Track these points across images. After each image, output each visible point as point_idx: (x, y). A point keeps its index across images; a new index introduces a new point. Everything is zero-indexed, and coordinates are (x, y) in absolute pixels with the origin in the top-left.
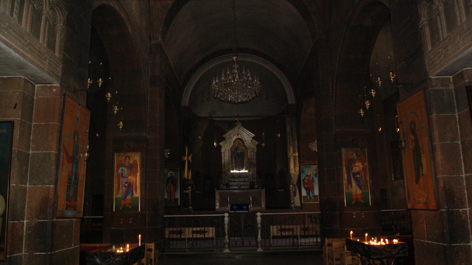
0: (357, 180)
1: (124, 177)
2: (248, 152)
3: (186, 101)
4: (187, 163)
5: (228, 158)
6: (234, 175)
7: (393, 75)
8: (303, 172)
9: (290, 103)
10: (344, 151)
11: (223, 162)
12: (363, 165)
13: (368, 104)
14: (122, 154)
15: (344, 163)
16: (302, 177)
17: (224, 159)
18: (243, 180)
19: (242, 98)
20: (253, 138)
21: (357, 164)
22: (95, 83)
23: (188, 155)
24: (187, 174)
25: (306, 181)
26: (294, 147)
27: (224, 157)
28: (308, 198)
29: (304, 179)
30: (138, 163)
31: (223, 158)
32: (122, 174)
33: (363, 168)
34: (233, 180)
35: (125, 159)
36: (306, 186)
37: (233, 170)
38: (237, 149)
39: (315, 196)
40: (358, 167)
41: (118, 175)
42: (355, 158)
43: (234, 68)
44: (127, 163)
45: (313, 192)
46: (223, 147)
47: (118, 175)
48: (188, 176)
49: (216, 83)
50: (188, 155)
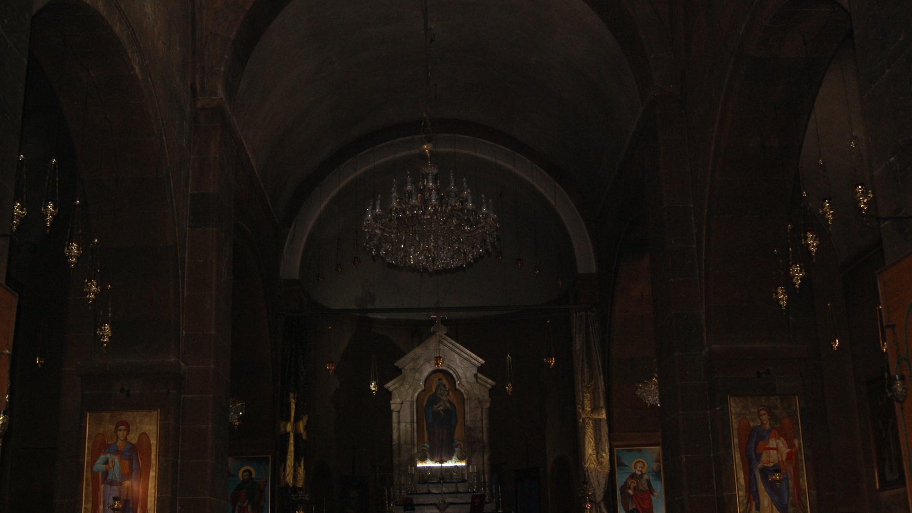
0: (772, 488)
1: (112, 483)
2: (467, 409)
3: (291, 266)
4: (292, 441)
5: (409, 426)
6: (426, 476)
7: (865, 194)
8: (621, 464)
9: (581, 269)
10: (734, 406)
11: (395, 436)
12: (790, 445)
13: (797, 273)
14: (107, 415)
15: (736, 440)
16: (620, 481)
17: (399, 430)
18: (452, 488)
19: (445, 259)
20: (481, 369)
21: (772, 443)
22: (35, 215)
23: (297, 419)
24: (293, 472)
25: (631, 492)
26: (594, 392)
27: (399, 423)
29: (625, 488)
30: (153, 442)
31: (395, 425)
32: (106, 473)
33: (789, 455)
34: (423, 488)
35: (116, 430)
37: (423, 460)
38: (434, 400)
40: (776, 450)
41: (95, 475)
42: (767, 426)
43: (425, 176)
44: (120, 443)
46: (395, 394)
47: (95, 475)
48: (295, 477)
49: (376, 218)
50: (297, 419)
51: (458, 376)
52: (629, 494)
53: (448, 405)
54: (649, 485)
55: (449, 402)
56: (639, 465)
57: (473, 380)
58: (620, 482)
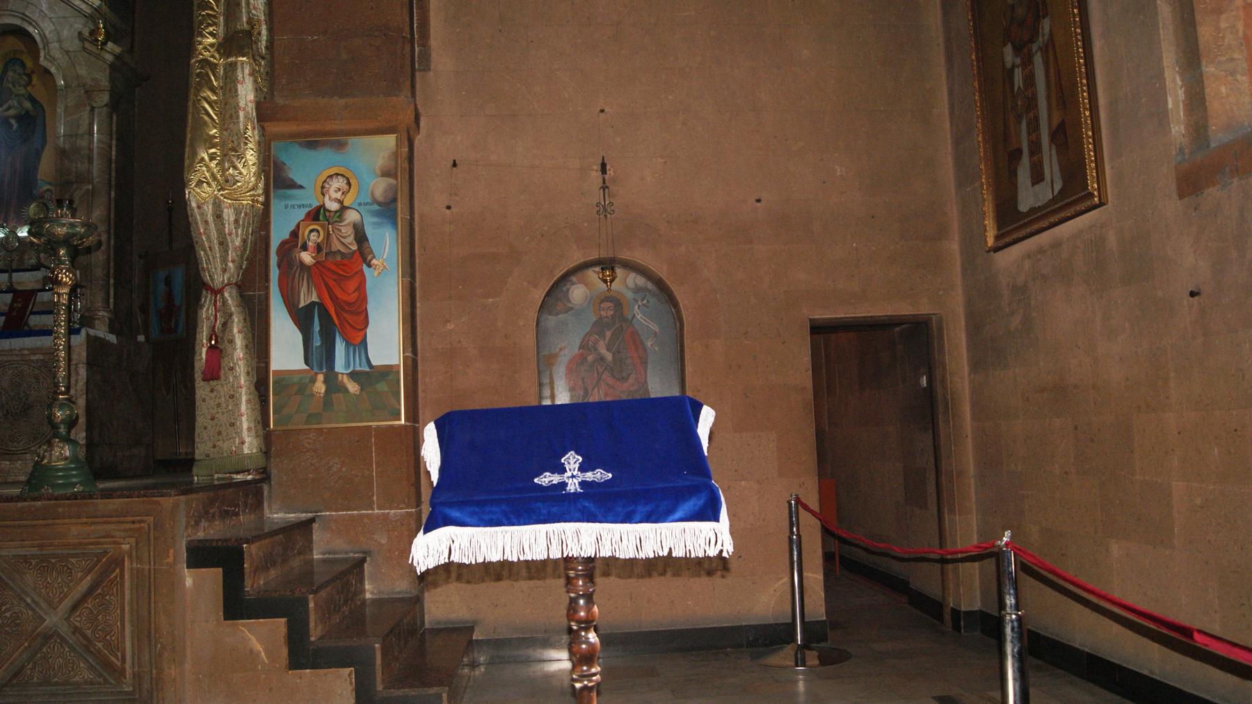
25: (307, 258)
28: (320, 387)
36: (307, 296)
39: (372, 377)
45: (364, 343)
51: (43, 36)
52: (302, 263)
53: (28, 105)
54: (361, 237)
55: (32, 99)
56: (338, 183)
57: (75, 45)
58: (279, 234)
